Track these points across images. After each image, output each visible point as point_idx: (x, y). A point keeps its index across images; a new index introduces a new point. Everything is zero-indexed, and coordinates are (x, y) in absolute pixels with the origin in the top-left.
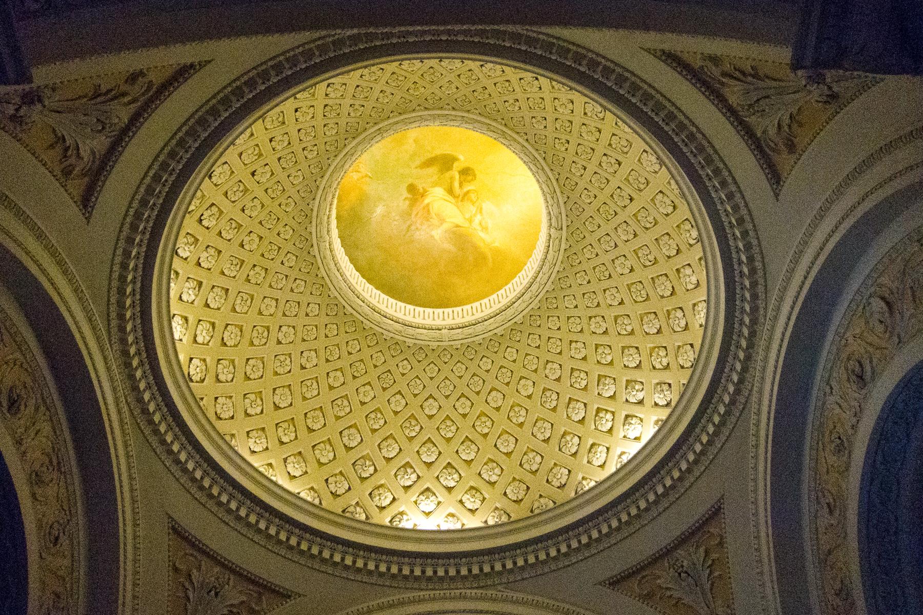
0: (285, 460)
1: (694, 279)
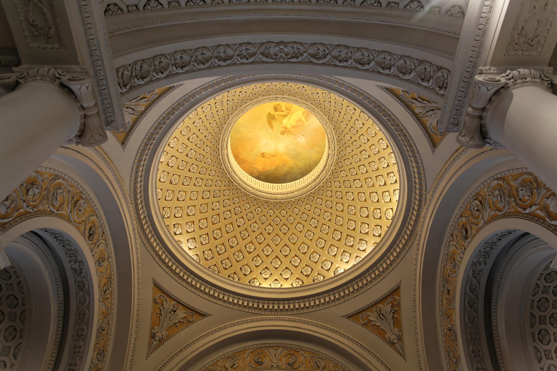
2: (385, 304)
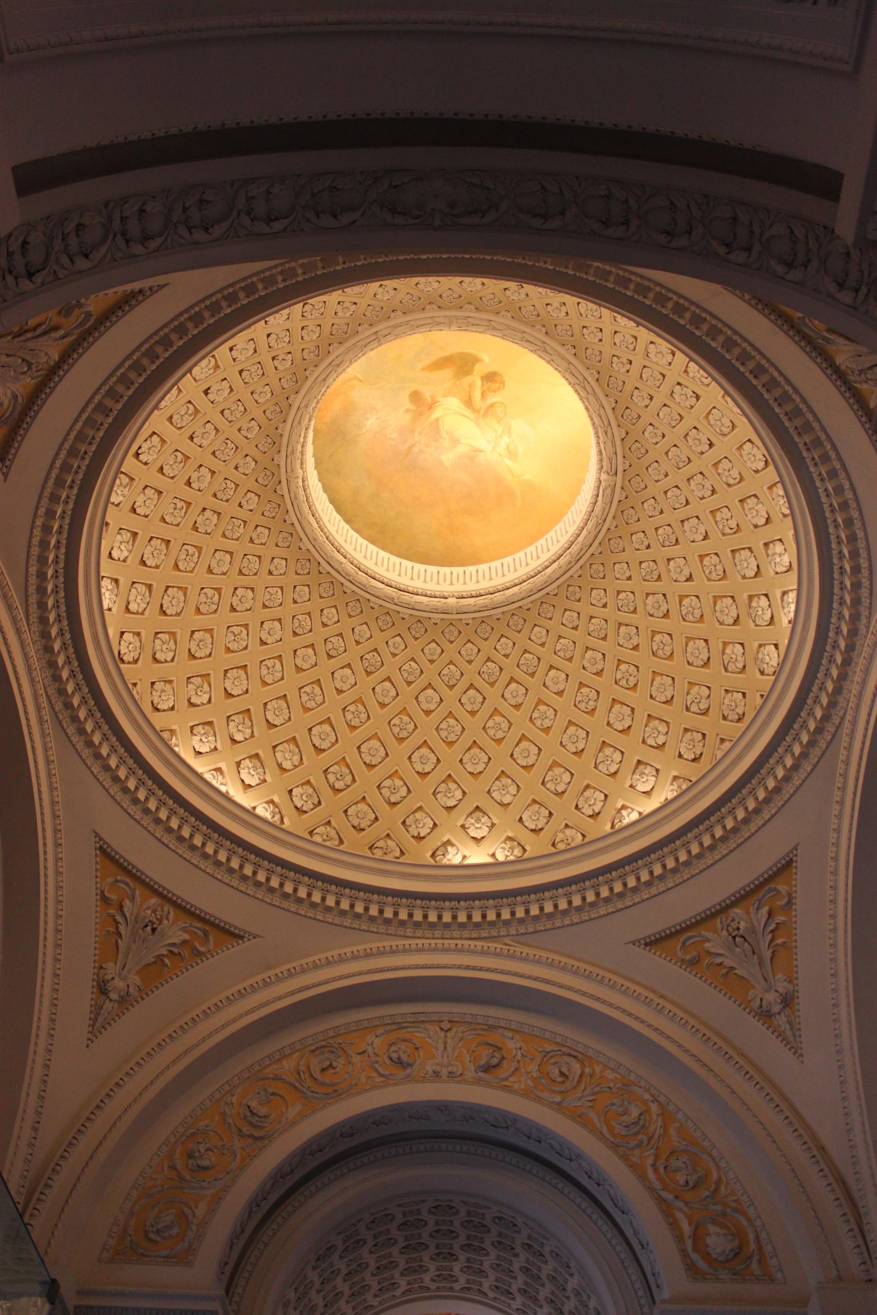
0: (238, 764)
1: (786, 560)
2: (181, 924)
